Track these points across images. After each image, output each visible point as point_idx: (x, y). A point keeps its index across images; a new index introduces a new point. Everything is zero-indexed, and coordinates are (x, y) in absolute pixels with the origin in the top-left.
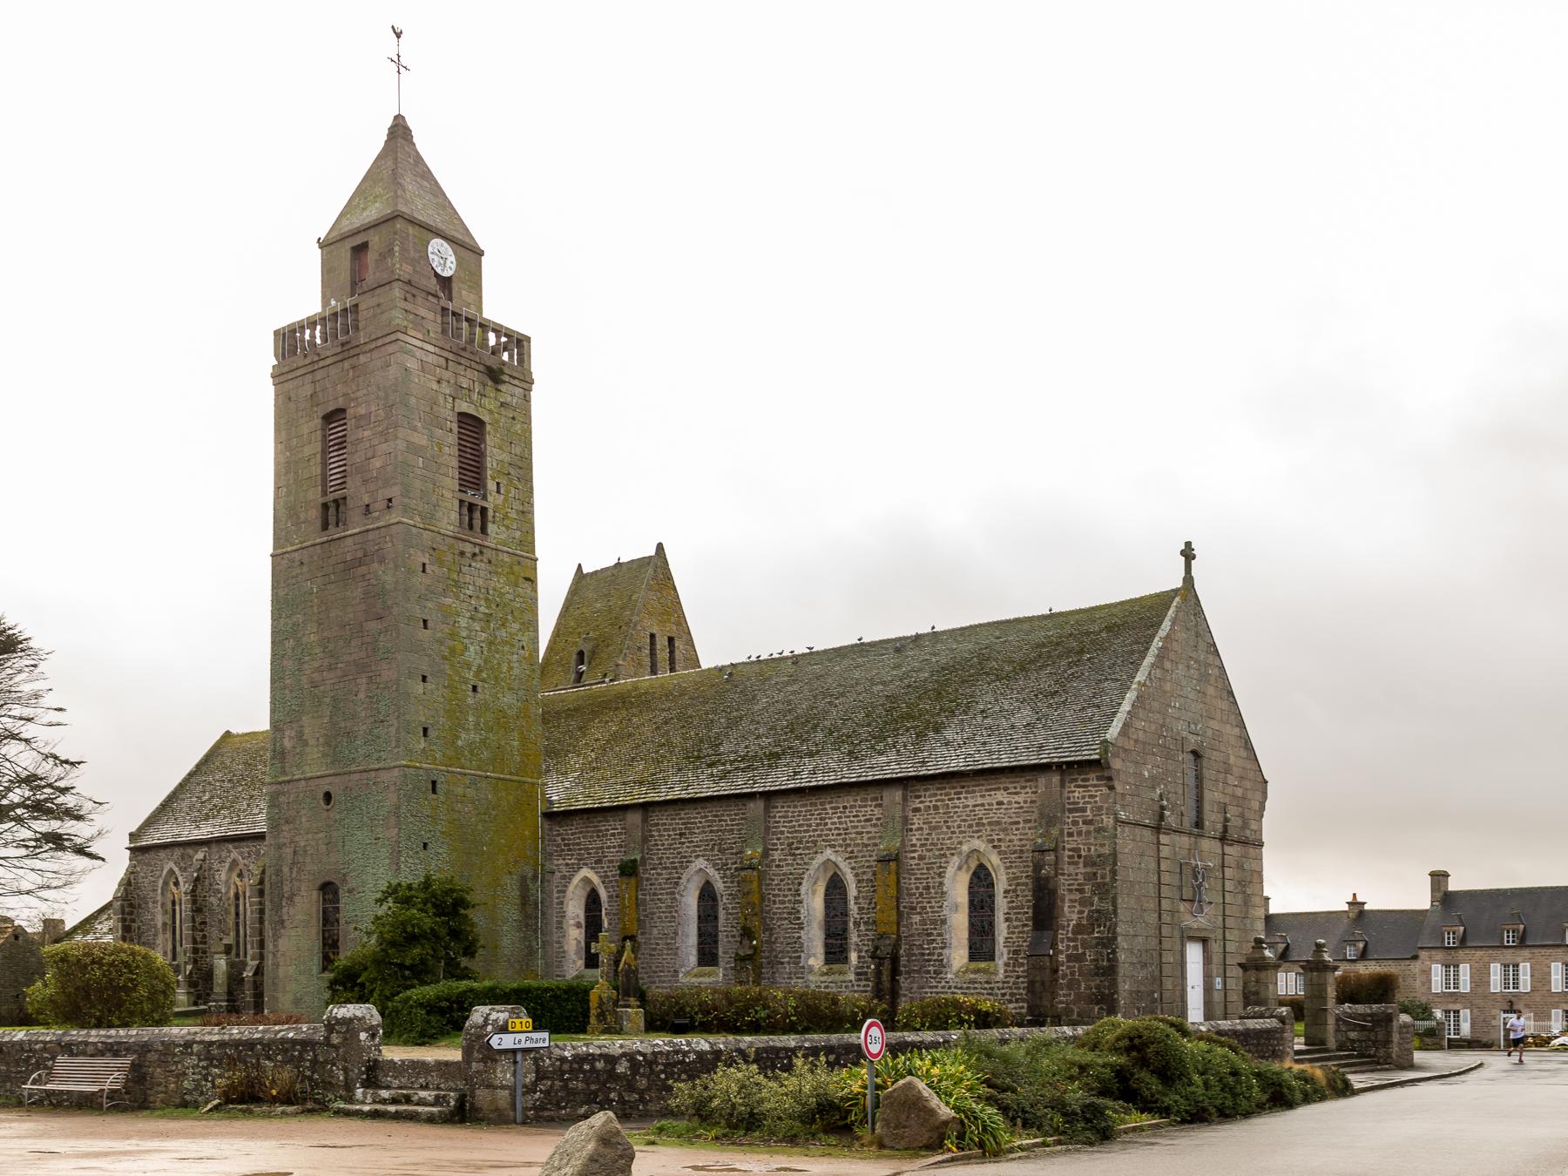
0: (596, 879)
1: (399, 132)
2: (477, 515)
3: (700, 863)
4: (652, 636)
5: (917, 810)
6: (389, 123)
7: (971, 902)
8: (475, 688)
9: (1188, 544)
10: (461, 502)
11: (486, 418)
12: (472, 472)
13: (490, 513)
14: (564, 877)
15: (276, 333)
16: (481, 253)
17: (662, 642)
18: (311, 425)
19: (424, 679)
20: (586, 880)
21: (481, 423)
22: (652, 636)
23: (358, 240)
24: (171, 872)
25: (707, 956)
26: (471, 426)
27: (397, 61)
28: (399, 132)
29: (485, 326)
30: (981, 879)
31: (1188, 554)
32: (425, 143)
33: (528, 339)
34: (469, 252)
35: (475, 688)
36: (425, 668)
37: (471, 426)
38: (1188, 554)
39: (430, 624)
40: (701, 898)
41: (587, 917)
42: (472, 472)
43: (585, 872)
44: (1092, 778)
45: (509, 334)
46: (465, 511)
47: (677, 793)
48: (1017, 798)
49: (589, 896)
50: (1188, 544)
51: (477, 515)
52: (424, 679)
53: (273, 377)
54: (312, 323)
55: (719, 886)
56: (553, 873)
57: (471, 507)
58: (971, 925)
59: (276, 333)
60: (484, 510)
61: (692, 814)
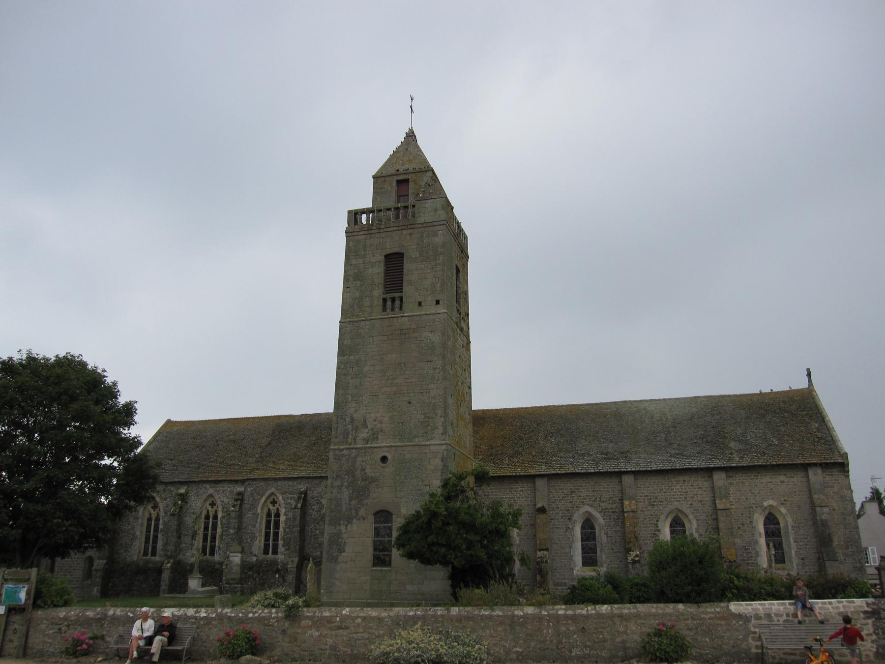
1: (411, 136)
3: (589, 509)
7: (766, 532)
9: (808, 370)
15: (349, 212)
25: (589, 560)
28: (411, 136)
30: (771, 520)
31: (809, 374)
38: (809, 374)
40: (583, 528)
44: (835, 472)
50: (808, 370)
55: (600, 520)
59: (349, 212)
61: (579, 482)
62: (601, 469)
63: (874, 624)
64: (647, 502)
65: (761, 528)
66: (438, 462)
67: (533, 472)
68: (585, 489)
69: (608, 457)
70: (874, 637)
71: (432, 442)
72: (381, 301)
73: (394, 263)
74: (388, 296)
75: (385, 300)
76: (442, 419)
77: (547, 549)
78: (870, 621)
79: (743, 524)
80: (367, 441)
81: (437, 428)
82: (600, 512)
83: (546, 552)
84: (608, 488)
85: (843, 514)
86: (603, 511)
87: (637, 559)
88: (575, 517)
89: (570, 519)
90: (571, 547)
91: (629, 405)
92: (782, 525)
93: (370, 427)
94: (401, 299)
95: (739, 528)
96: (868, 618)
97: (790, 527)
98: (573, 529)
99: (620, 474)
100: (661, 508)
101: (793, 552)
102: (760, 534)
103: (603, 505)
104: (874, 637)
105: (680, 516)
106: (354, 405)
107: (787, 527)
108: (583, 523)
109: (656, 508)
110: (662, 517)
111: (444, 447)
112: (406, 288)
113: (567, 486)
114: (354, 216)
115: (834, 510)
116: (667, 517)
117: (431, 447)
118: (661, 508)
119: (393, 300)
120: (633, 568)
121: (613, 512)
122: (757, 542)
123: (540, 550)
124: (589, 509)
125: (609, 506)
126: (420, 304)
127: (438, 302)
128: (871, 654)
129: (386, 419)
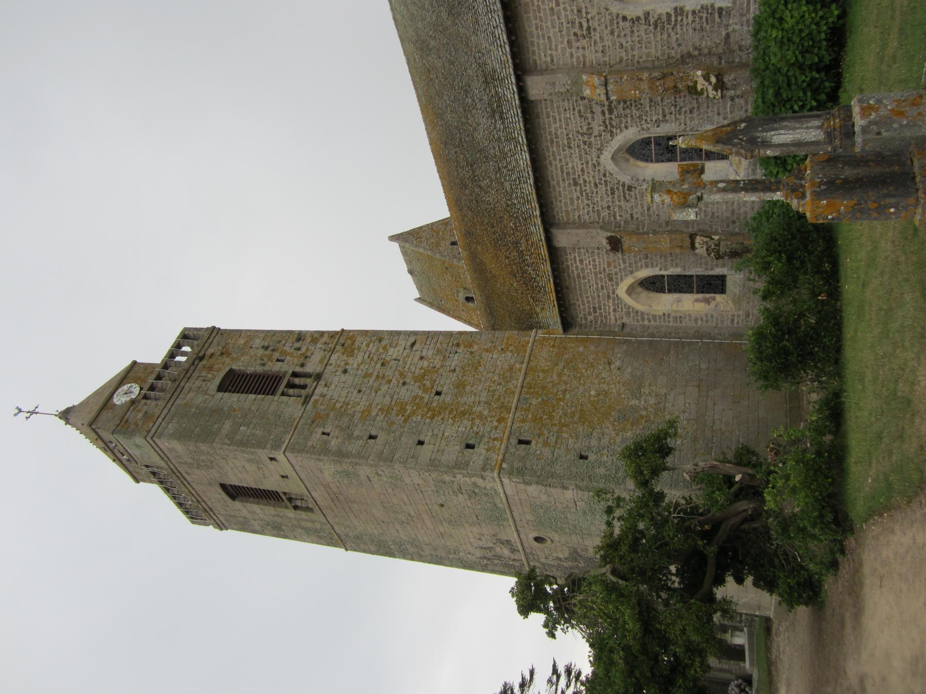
0: (629, 281)
2: (297, 381)
3: (606, 158)
6: (63, 422)
8: (438, 393)
10: (283, 394)
11: (227, 369)
12: (264, 384)
13: (298, 369)
14: (628, 314)
16: (135, 363)
18: (241, 508)
19: (421, 443)
20: (630, 291)
21: (231, 371)
26: (235, 382)
27: (32, 413)
29: (165, 366)
32: (76, 399)
33: (185, 329)
34: (133, 372)
35: (438, 393)
36: (408, 440)
37: (235, 382)
39: (374, 433)
40: (647, 159)
41: (670, 291)
42: (264, 384)
43: (621, 291)
45: (178, 346)
46: (291, 391)
47: (529, 188)
49: (647, 289)
51: (297, 381)
52: (421, 443)
55: (631, 134)
56: (623, 325)
60: (295, 375)
61: (554, 171)
62: (522, 139)
64: (584, 42)
66: (533, 490)
67: (544, 251)
68: (563, 161)
69: (496, 111)
71: (501, 491)
72: (298, 512)
73: (234, 492)
76: (459, 476)
77: (692, 237)
80: (513, 550)
81: (475, 484)
82: (612, 135)
83: (698, 240)
84: (558, 124)
86: (610, 129)
87: (713, 80)
88: (626, 179)
89: (630, 188)
91: (398, 17)
93: (492, 545)
99: (527, 107)
100: (593, 12)
103: (597, 128)
109: (594, 24)
111: (506, 481)
113: (566, 199)
117: (509, 492)
118: (593, 12)
119: (290, 499)
120: (735, 87)
121: (611, 112)
123: (693, 247)
124: (606, 158)
125: (599, 118)
127: (271, 459)
129: (475, 529)
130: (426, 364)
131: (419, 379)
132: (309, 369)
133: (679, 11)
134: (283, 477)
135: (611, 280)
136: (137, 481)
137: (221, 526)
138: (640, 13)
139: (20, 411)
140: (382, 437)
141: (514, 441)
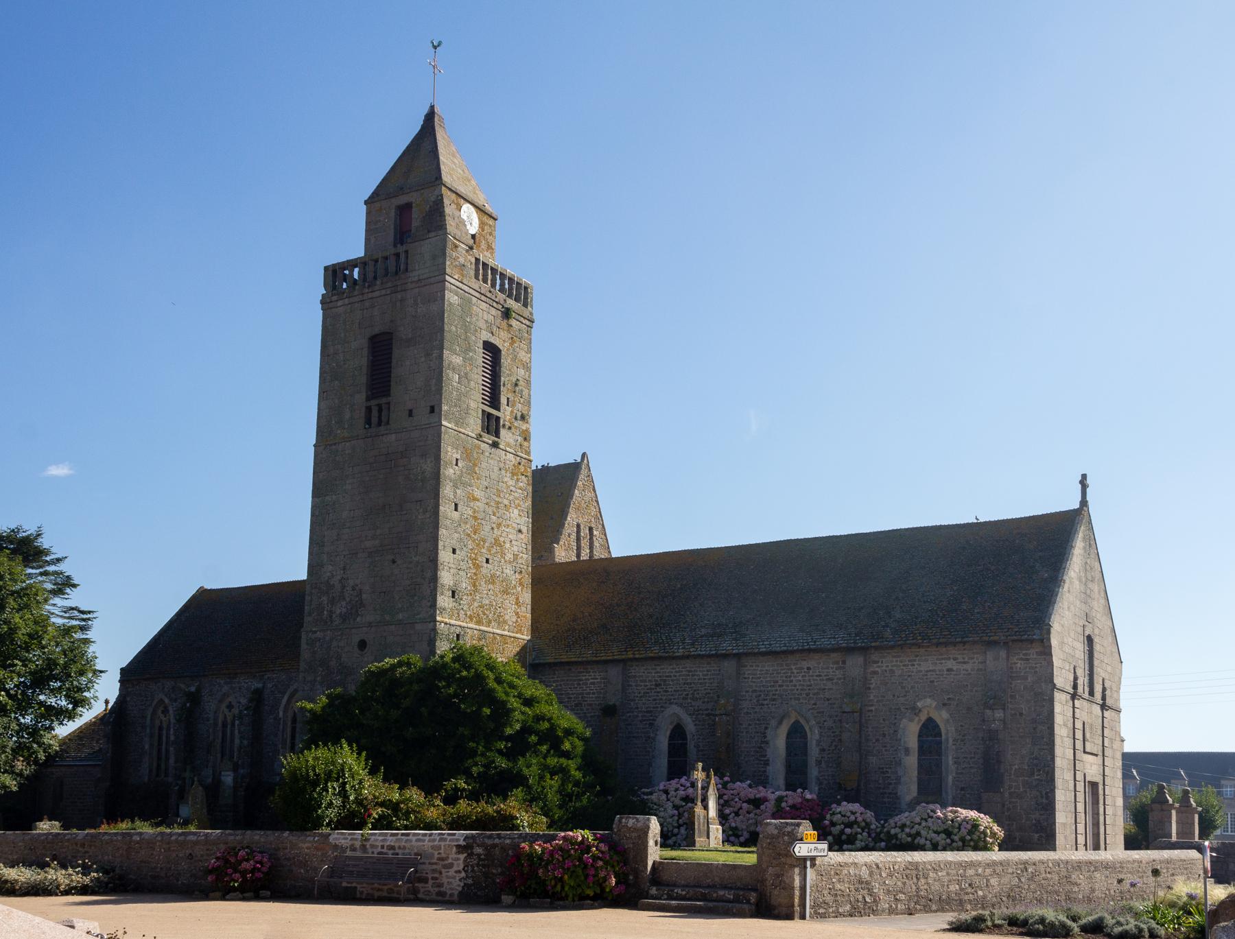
4: (578, 526)
5: (875, 673)
7: (921, 748)
8: (487, 561)
15: (326, 269)
17: (585, 532)
19: (454, 551)
22: (578, 526)
23: (402, 200)
24: (162, 701)
35: (487, 561)
40: (671, 738)
48: (965, 666)
52: (454, 551)
53: (322, 302)
54: (352, 264)
57: (489, 415)
58: (920, 766)
59: (326, 269)
60: (498, 419)
63: (465, 861)
65: (912, 742)
70: (463, 874)
72: (363, 410)
73: (381, 351)
74: (373, 403)
75: (369, 409)
78: (462, 856)
79: (884, 735)
85: (1034, 721)
89: (651, 724)
90: (650, 765)
92: (944, 737)
94: (389, 403)
95: (877, 740)
96: (459, 853)
97: (951, 741)
98: (654, 739)
101: (950, 778)
102: (907, 751)
104: (463, 874)
105: (802, 721)
106: (330, 568)
107: (947, 740)
108: (673, 730)
110: (773, 723)
112: (396, 390)
114: (335, 274)
115: (1021, 714)
116: (780, 723)
121: (708, 715)
122: (899, 763)
126: (410, 413)
128: (456, 893)
130: (508, 545)
131: (496, 542)
132: (503, 432)
133: (767, 763)
134: (411, 411)
135: (576, 705)
136: (366, 202)
137: (324, 302)
138: (769, 738)
139: (435, 47)
140: (456, 515)
141: (458, 630)
